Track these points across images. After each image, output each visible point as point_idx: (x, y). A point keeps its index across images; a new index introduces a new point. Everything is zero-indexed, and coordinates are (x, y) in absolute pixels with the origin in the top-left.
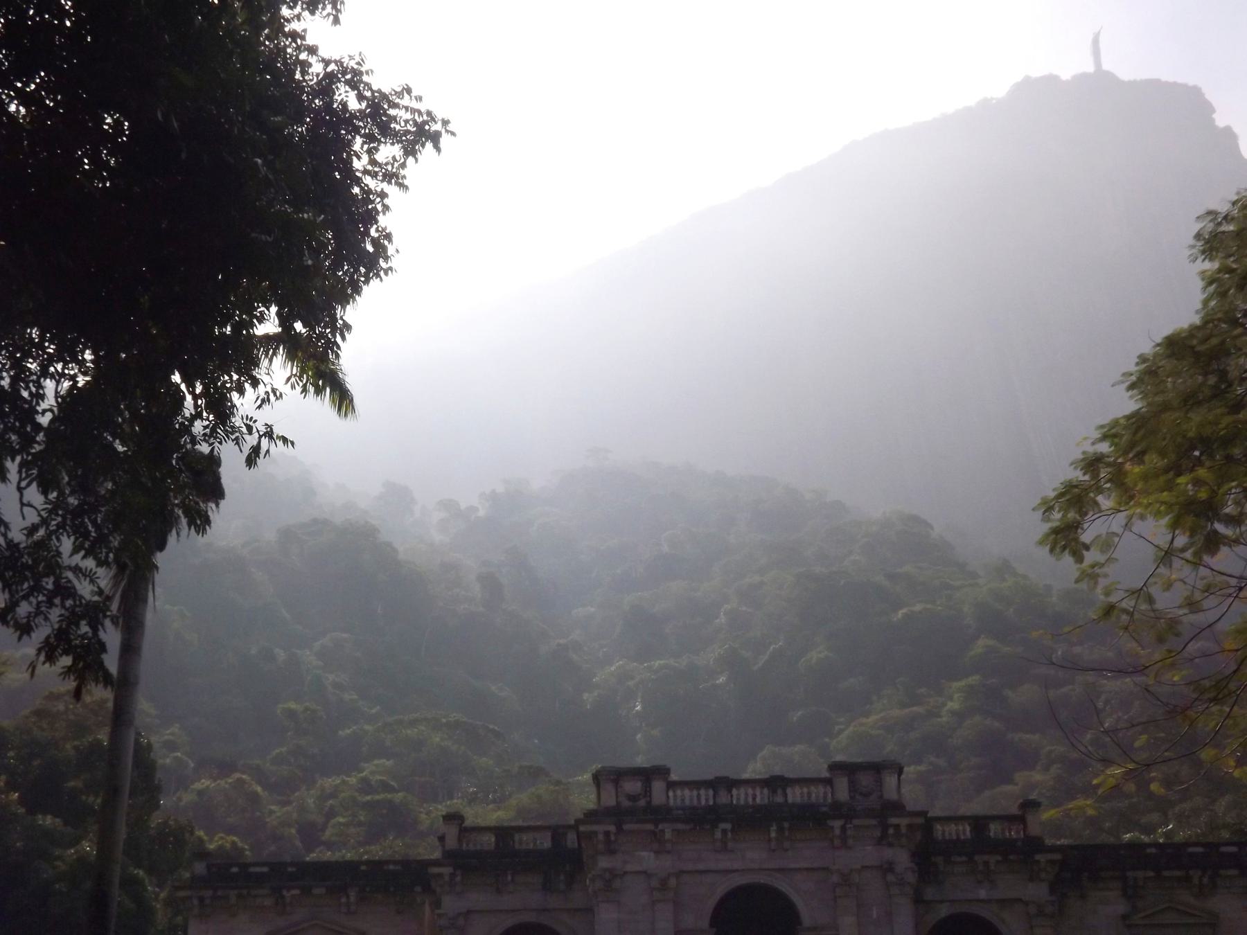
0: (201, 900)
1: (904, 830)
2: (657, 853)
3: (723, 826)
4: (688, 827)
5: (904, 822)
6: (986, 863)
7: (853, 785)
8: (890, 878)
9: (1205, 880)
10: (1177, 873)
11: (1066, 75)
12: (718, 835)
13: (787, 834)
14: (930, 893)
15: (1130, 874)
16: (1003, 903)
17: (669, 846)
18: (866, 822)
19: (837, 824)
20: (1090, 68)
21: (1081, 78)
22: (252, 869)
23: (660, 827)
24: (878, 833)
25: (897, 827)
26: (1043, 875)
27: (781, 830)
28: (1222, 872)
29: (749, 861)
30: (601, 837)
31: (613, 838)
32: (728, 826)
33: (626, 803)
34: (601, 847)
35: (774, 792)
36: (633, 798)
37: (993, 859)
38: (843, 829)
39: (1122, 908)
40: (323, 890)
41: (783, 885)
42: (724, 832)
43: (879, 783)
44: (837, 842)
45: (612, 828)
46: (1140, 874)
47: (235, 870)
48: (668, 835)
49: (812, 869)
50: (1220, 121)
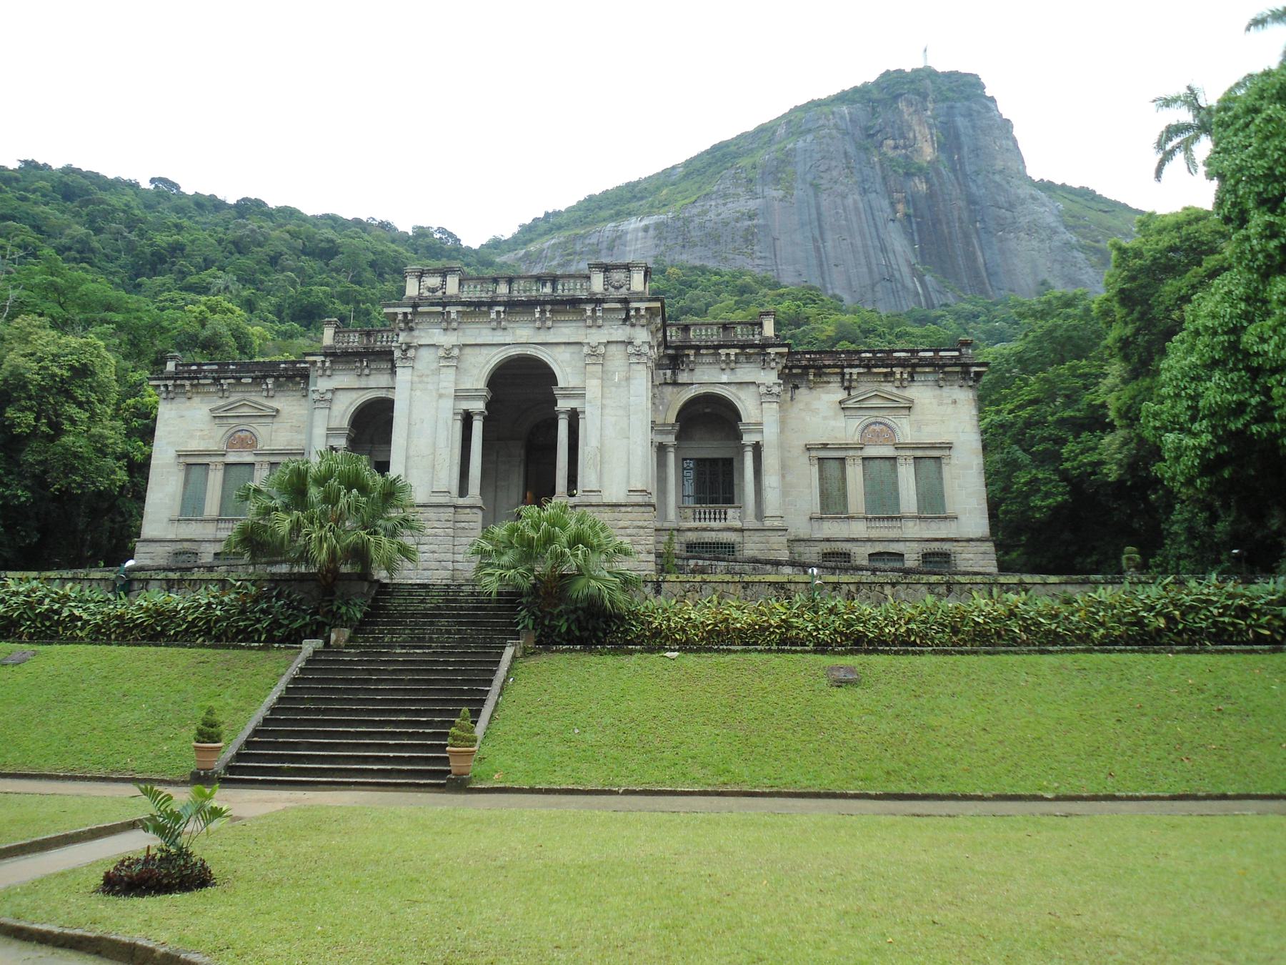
0: (166, 386)
1: (643, 312)
2: (445, 330)
5: (643, 305)
7: (607, 281)
8: (630, 349)
9: (905, 376)
10: (885, 370)
11: (908, 70)
12: (493, 316)
13: (548, 315)
14: (683, 377)
15: (847, 370)
17: (454, 325)
19: (589, 308)
20: (921, 66)
21: (915, 71)
25: (638, 310)
26: (773, 364)
27: (543, 312)
28: (918, 369)
29: (521, 337)
30: (400, 317)
31: (409, 317)
32: (502, 309)
33: (427, 294)
34: (402, 325)
35: (544, 285)
36: (433, 290)
37: (733, 351)
38: (594, 311)
39: (842, 395)
40: (250, 380)
41: (543, 354)
42: (498, 312)
43: (629, 278)
44: (589, 322)
45: (409, 310)
46: (855, 371)
47: (194, 368)
48: (453, 316)
50: (988, 93)
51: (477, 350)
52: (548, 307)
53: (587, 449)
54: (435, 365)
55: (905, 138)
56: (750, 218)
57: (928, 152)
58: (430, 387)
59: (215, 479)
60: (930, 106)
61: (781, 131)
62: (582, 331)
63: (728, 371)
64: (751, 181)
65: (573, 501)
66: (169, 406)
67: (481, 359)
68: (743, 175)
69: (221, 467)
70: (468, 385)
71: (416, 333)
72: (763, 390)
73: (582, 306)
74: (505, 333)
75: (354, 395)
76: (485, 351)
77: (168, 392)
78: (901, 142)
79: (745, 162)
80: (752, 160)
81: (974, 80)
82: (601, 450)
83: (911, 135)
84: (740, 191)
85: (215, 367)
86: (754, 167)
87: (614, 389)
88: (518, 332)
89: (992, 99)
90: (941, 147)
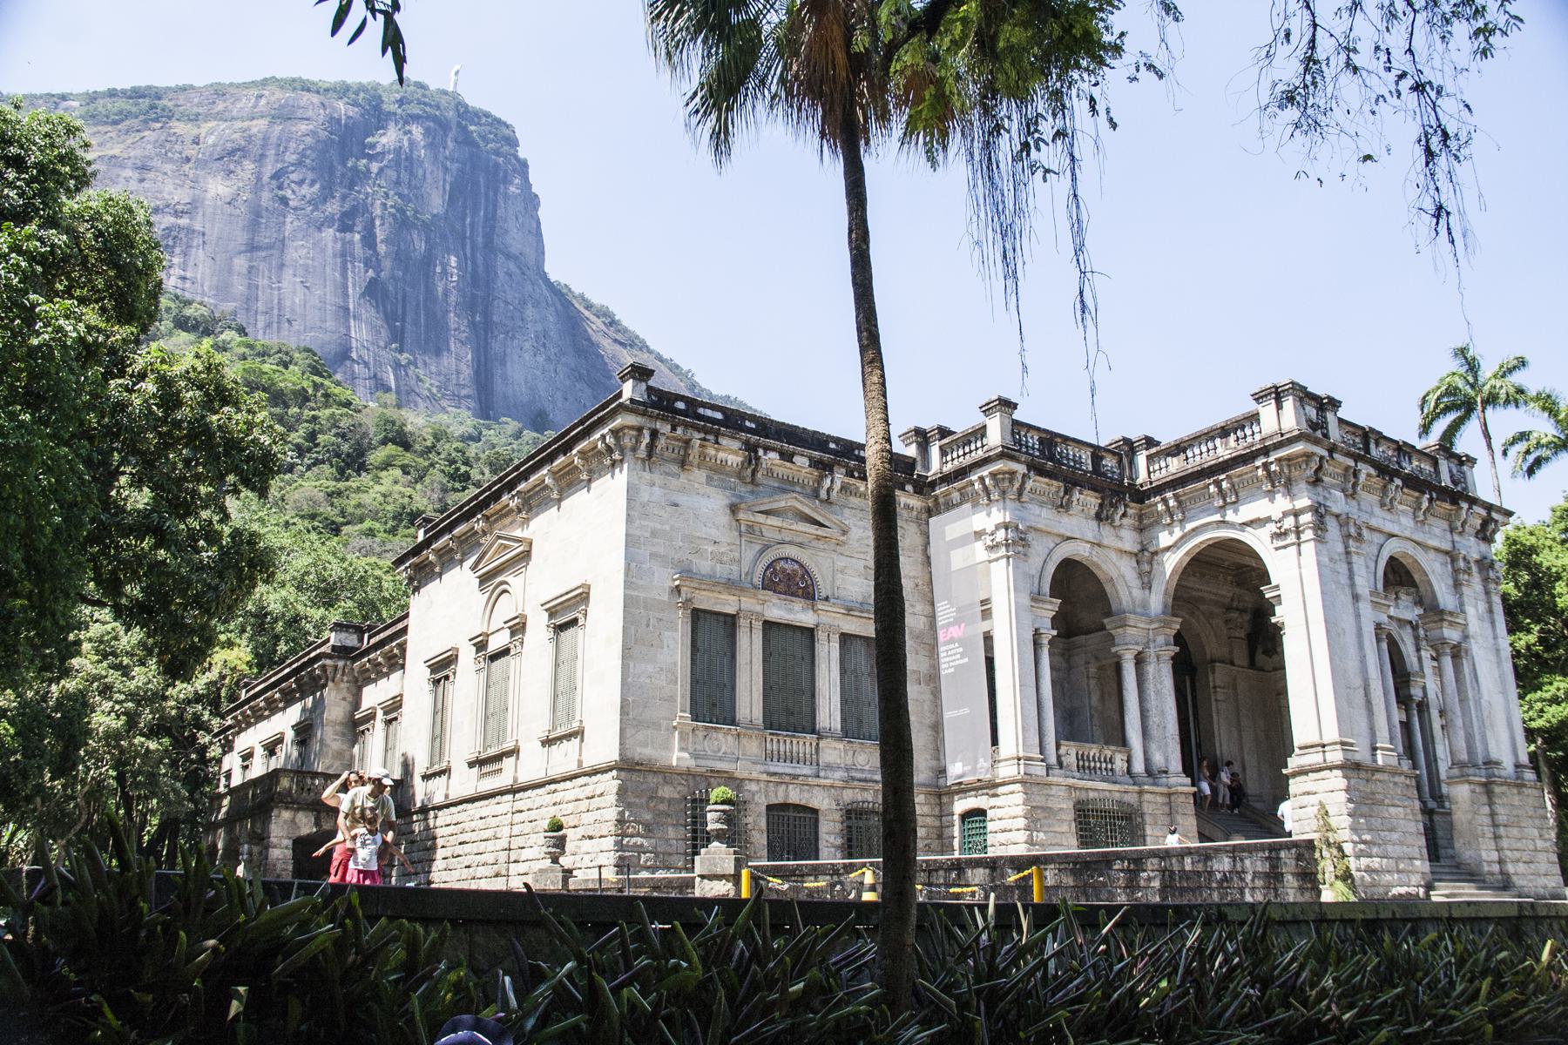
0: (654, 434)
22: (701, 411)
50: (522, 154)
55: (411, 173)
56: (177, 214)
57: (436, 203)
59: (750, 648)
60: (450, 144)
61: (245, 103)
64: (188, 160)
66: (647, 475)
68: (178, 147)
69: (758, 625)
77: (651, 447)
78: (405, 176)
79: (179, 127)
80: (196, 131)
81: (506, 132)
83: (420, 172)
84: (168, 167)
85: (719, 416)
86: (196, 142)
89: (524, 166)
90: (452, 201)
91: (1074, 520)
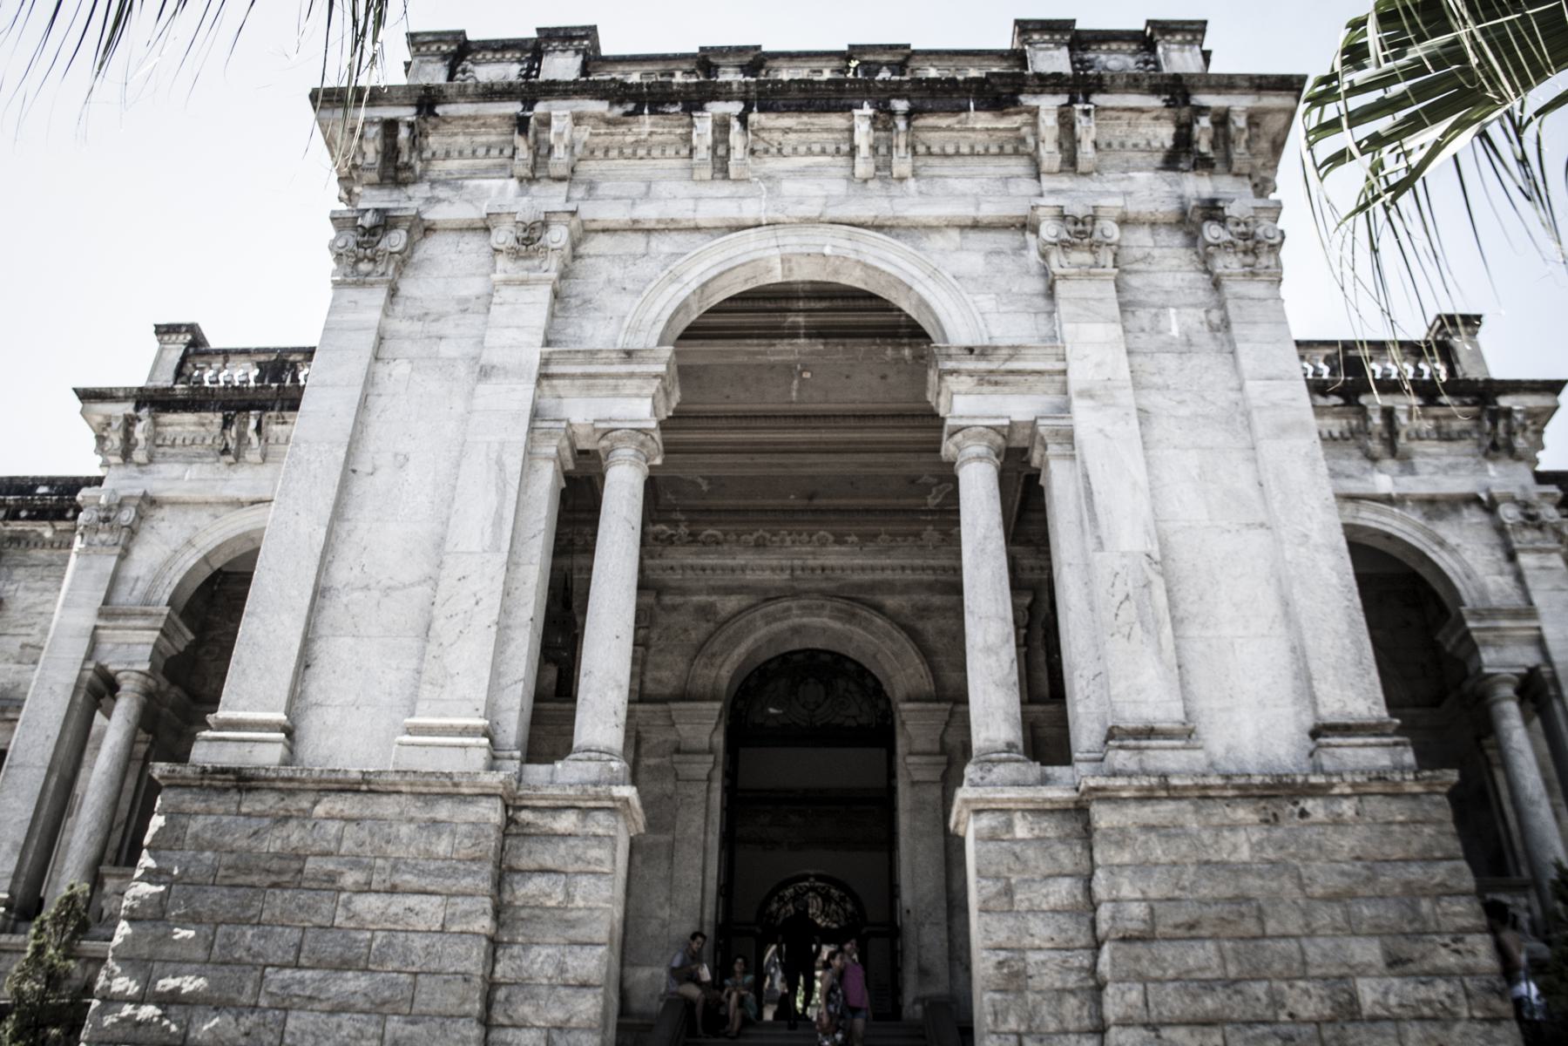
3: (717, 108)
4: (618, 111)
5: (1238, 103)
6: (1388, 414)
8: (1212, 232)
12: (704, 125)
16: (1434, 506)
18: (1134, 100)
23: (540, 108)
24: (1165, 134)
27: (883, 119)
31: (404, 133)
32: (736, 107)
38: (1066, 123)
44: (1050, 154)
45: (407, 113)
49: (976, 226)
51: (637, 243)
52: (901, 105)
53: (1106, 563)
54: (476, 286)
58: (447, 349)
62: (1027, 186)
63: (1389, 463)
65: (1061, 786)
67: (647, 268)
70: (597, 332)
71: (420, 191)
72: (1508, 513)
73: (1027, 100)
74: (742, 189)
75: (203, 518)
76: (663, 245)
82: (1162, 561)
87: (1170, 361)
88: (789, 187)
91: (267, 471)
